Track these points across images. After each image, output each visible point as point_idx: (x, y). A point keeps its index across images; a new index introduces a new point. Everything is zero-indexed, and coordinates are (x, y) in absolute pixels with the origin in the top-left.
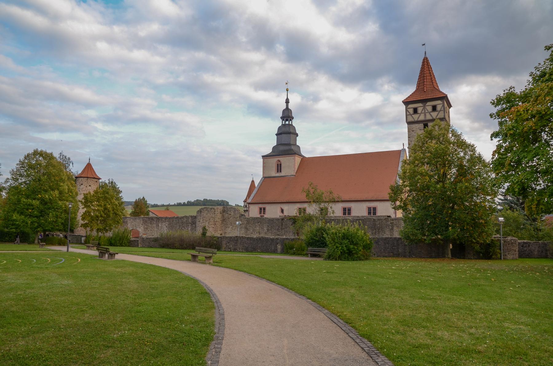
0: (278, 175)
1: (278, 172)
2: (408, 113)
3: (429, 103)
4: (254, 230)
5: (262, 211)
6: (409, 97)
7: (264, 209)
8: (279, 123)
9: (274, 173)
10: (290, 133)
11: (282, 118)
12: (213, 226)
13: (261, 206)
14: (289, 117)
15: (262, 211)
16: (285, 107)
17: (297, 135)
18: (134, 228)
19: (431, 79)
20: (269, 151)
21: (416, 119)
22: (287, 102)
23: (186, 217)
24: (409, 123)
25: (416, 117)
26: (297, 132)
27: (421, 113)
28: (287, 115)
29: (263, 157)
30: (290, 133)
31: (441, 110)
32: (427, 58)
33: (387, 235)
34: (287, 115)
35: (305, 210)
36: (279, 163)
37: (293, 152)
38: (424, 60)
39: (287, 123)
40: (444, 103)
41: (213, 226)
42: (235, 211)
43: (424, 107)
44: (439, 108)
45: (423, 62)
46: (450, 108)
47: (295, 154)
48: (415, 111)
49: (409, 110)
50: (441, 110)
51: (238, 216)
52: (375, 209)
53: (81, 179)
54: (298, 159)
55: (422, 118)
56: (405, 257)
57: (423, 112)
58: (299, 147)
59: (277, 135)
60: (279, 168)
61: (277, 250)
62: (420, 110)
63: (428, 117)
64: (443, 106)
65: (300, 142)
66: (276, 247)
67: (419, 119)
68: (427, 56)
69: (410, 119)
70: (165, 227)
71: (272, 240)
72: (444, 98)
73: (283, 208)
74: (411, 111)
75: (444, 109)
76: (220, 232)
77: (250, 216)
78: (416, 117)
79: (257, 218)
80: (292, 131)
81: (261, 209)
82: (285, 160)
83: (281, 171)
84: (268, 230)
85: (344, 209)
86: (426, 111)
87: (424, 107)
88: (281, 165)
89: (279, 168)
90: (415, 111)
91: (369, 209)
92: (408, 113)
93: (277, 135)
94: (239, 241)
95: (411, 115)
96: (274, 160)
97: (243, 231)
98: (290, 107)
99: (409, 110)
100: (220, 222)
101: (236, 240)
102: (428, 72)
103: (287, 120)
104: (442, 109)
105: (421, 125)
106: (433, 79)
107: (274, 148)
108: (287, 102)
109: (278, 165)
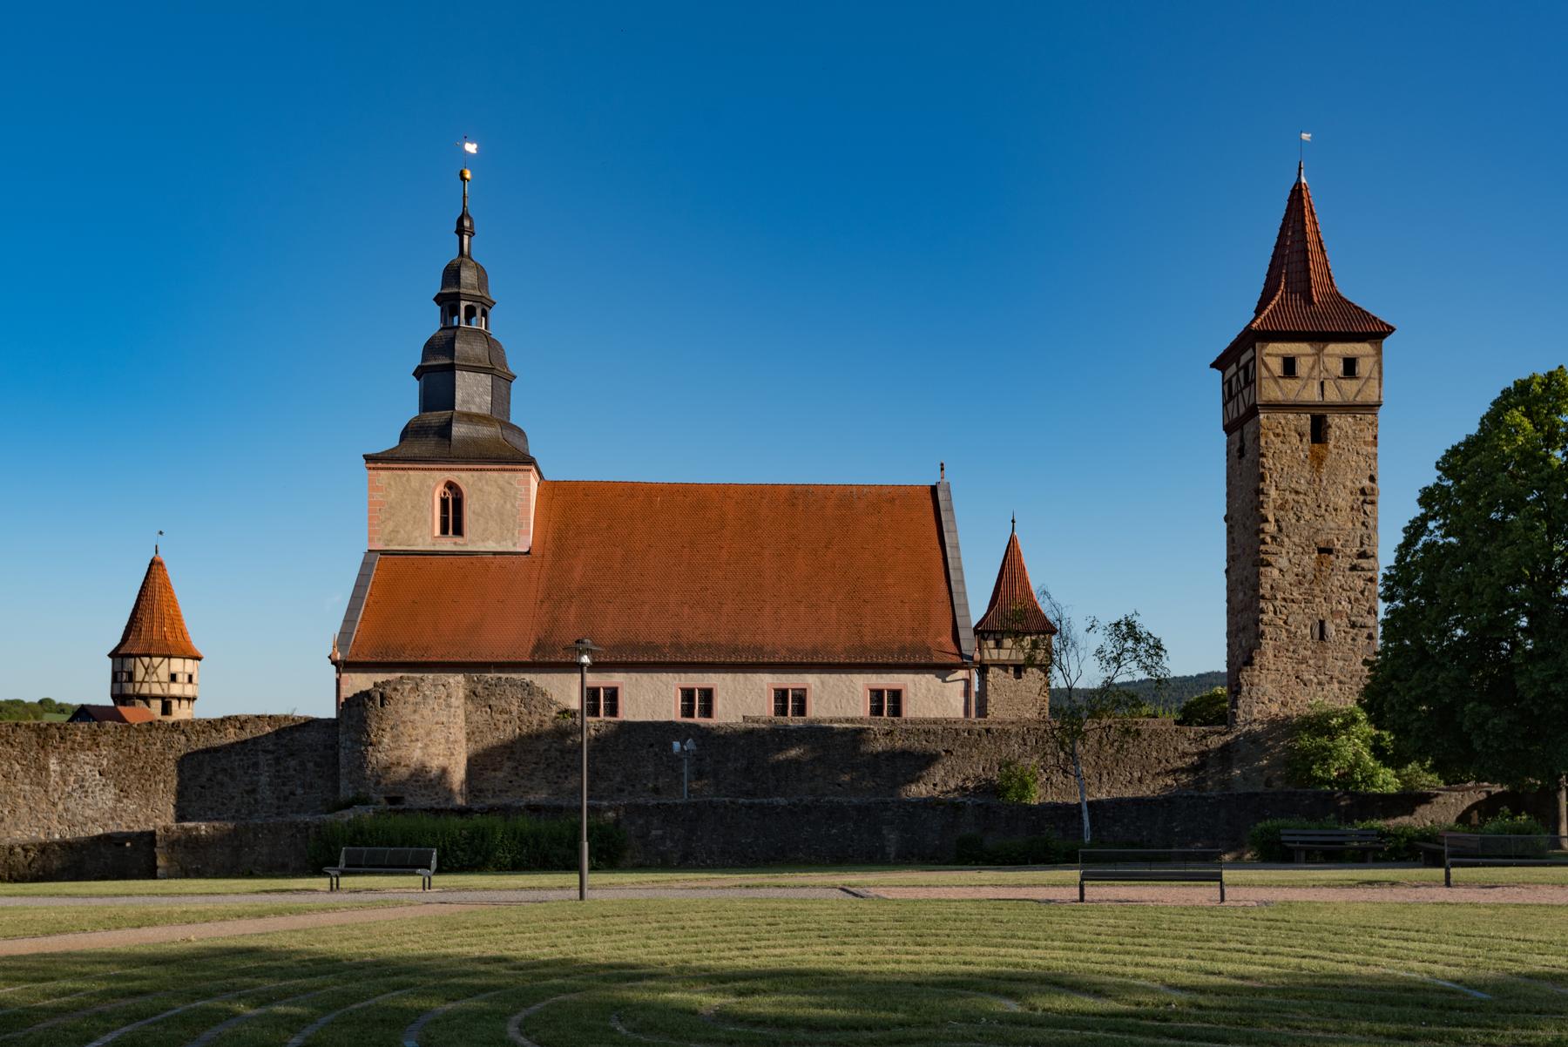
0: (449, 544)
9: (427, 535)
21: (1292, 398)
26: (513, 369)
35: (801, 700)
48: (1289, 366)
52: (896, 695)
55: (1312, 394)
57: (1316, 372)
58: (521, 432)
60: (453, 516)
63: (1332, 396)
82: (481, 487)
89: (453, 516)
90: (1289, 366)
95: (1275, 379)
96: (430, 484)
105: (1305, 421)
109: (444, 502)
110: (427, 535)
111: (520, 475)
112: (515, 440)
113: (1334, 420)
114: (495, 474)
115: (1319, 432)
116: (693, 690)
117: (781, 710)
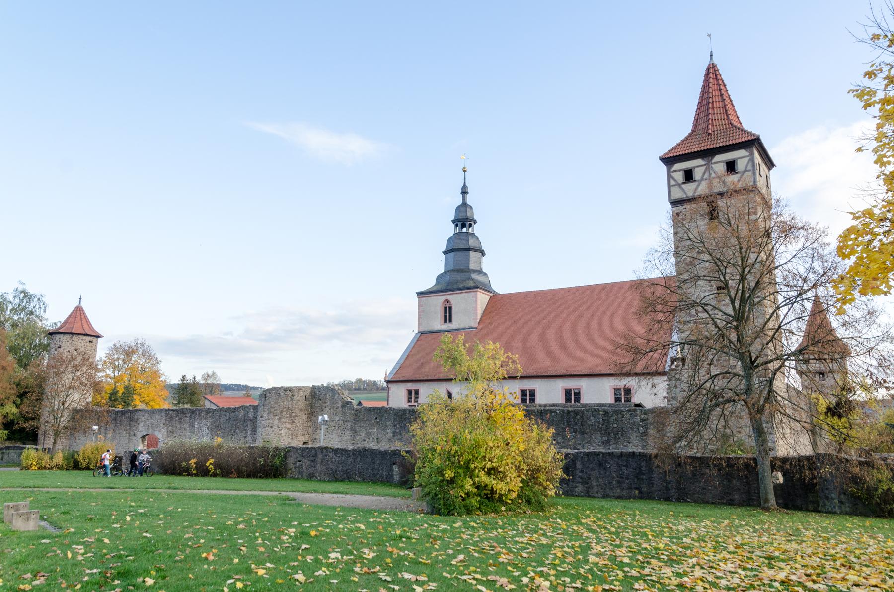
0: (445, 327)
1: (445, 321)
2: (673, 183)
3: (718, 158)
4: (368, 434)
5: (413, 395)
6: (674, 148)
7: (417, 392)
8: (450, 230)
9: (437, 324)
10: (468, 249)
11: (455, 222)
12: (288, 426)
13: (410, 386)
14: (467, 219)
15: (413, 395)
16: (460, 202)
17: (483, 254)
18: (150, 432)
19: (722, 95)
20: (429, 283)
21: (690, 194)
22: (464, 192)
23: (244, 408)
24: (675, 203)
25: (690, 189)
26: (483, 248)
27: (702, 179)
28: (464, 220)
29: (419, 294)
30: (468, 249)
31: (746, 171)
32: (714, 66)
33: (634, 447)
34: (464, 220)
36: (448, 306)
37: (471, 284)
38: (708, 69)
39: (464, 230)
40: (752, 154)
41: (288, 426)
42: (333, 395)
43: (708, 166)
44: (740, 166)
45: (707, 75)
46: (769, 169)
47: (476, 287)
48: (689, 176)
49: (674, 175)
50: (746, 171)
51: (340, 404)
53: (58, 336)
54: (482, 298)
56: (667, 499)
57: (706, 176)
58: (485, 274)
59: (445, 253)
60: (448, 314)
61: (392, 476)
62: (698, 174)
63: (718, 188)
64: (752, 160)
65: (487, 264)
66: (392, 470)
67: (697, 194)
68: (715, 61)
69: (678, 194)
70: (205, 428)
71: (383, 454)
72: (754, 143)
73: (450, 391)
74: (680, 177)
75: (754, 166)
76: (303, 439)
77: (390, 406)
78: (690, 189)
79: (404, 410)
80: (472, 243)
81: (410, 392)
82: (458, 300)
83: (450, 321)
84: (394, 432)
85: (568, 392)
86: (713, 175)
87: (708, 166)
88: (450, 308)
89: (448, 314)
90: (689, 176)
91: (617, 390)
92: (673, 183)
93: (445, 253)
94: (320, 457)
95: (679, 185)
96: (438, 301)
97: (347, 436)
98: (469, 202)
99: (674, 175)
100: (305, 417)
101: (310, 454)
102: (717, 93)
103: (463, 226)
104: (750, 167)
106: (729, 106)
107: (439, 277)
108: (464, 192)
109: (445, 308)
110: (437, 324)
111: (473, 294)
112: (480, 278)
113: (721, 203)
114: (463, 295)
115: (713, 214)
116: (570, 390)
117: (568, 400)
